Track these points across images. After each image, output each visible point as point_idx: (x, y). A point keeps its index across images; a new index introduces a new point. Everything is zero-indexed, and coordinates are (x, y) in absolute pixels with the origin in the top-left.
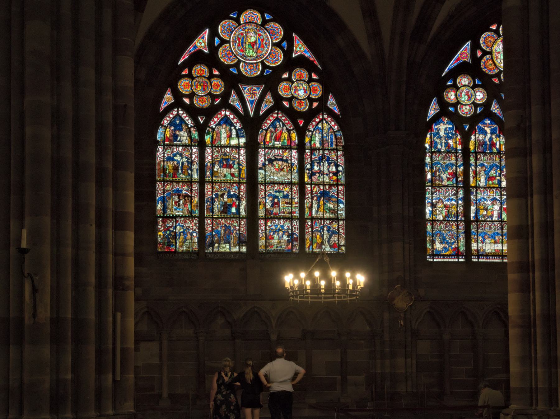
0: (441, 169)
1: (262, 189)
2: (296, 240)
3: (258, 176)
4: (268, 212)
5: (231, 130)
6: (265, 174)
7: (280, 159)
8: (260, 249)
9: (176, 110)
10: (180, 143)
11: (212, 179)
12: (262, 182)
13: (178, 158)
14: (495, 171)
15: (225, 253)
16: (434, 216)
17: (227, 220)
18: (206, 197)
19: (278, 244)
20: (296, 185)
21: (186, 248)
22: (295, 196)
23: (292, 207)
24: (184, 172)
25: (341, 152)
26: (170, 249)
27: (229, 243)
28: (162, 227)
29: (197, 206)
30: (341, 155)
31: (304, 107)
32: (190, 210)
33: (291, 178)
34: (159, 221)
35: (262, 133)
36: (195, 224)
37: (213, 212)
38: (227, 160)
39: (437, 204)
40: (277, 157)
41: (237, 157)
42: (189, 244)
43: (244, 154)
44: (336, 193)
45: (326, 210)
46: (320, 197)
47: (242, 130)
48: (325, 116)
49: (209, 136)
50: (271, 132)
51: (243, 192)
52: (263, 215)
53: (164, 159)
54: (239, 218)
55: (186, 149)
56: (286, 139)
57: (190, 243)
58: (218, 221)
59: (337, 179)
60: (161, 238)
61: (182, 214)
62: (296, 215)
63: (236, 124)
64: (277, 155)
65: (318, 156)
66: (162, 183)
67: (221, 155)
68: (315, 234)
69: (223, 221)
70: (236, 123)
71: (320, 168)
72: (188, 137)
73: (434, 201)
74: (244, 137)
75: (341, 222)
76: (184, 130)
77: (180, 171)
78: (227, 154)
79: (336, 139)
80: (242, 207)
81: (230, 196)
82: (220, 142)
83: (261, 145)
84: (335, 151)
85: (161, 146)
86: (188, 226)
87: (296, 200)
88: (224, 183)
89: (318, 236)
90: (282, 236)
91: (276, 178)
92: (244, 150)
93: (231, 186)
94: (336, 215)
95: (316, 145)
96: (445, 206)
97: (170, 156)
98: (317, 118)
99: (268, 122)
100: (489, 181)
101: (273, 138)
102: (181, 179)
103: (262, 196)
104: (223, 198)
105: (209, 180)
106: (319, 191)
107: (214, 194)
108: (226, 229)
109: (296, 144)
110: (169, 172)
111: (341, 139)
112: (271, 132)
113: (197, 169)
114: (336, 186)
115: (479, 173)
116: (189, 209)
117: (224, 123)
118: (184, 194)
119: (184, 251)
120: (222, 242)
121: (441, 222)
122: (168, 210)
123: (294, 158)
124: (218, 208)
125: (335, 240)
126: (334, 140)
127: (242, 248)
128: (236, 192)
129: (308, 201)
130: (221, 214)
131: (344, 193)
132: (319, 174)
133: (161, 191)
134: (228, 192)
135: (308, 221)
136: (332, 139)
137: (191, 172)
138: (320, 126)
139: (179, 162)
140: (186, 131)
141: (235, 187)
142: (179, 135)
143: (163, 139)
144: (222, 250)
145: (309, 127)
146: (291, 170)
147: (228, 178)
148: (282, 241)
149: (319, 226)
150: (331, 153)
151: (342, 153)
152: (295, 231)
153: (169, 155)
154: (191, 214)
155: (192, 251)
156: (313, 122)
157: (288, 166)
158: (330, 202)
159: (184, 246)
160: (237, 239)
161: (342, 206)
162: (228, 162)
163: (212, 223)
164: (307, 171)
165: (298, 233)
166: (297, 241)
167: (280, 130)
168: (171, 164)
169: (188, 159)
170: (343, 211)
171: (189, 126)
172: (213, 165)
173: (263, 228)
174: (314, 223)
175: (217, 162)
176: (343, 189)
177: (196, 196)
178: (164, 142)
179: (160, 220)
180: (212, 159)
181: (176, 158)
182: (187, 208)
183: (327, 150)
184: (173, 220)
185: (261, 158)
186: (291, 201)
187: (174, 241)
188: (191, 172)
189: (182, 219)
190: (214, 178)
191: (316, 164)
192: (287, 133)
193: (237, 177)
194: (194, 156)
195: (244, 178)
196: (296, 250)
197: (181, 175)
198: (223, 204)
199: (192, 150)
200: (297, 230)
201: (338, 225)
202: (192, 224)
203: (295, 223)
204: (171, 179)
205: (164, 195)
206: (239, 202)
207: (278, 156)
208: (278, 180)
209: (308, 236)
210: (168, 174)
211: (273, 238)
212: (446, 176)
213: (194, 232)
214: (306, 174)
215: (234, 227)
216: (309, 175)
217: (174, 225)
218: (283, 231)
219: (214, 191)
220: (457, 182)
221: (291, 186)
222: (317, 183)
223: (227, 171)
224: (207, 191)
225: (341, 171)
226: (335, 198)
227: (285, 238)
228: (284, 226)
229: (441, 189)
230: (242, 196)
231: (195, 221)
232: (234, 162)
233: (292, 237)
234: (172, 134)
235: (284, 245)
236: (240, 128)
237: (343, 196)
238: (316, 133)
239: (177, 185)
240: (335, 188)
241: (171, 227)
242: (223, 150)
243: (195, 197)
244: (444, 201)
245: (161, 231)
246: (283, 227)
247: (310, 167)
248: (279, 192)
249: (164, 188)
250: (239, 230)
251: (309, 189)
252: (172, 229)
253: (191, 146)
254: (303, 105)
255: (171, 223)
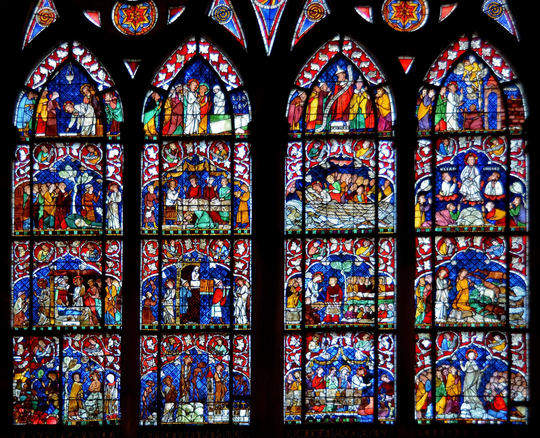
1: (294, 252)
2: (388, 389)
3: (283, 219)
4: (311, 315)
5: (211, 95)
6: (304, 211)
7: (345, 166)
8: (287, 415)
9: (65, 46)
10: (75, 134)
11: (160, 230)
12: (294, 232)
13: (68, 174)
15: (192, 427)
17: (197, 337)
18: (144, 277)
19: (338, 401)
20: (390, 239)
21: (89, 415)
22: (385, 270)
23: (376, 299)
24: (86, 213)
25: (520, 142)
26: (45, 420)
27: (204, 400)
28: (23, 359)
29: (118, 303)
30: (519, 150)
31: (415, 18)
32: (100, 312)
33: (377, 220)
34: (17, 344)
35: (297, 100)
36: (113, 349)
37: (160, 318)
38: (199, 175)
40: (336, 163)
41: (228, 167)
42: (97, 404)
43: (247, 159)
44: (503, 258)
45: (475, 305)
46: (458, 270)
47: (243, 94)
48: (476, 44)
49: (151, 113)
50: (322, 95)
51: (242, 262)
52: (297, 323)
53: (31, 178)
54: (231, 332)
55: (91, 150)
56: (364, 111)
57: (100, 402)
58: (173, 341)
59: (508, 214)
60: (21, 389)
61: (78, 323)
62: (390, 320)
63: (227, 78)
64: (337, 156)
65: (453, 152)
66: (27, 243)
67: (183, 164)
68: (442, 371)
69: (188, 339)
70: (226, 75)
71: (458, 188)
72: (97, 118)
74: (247, 112)
75: (517, 339)
76: (86, 100)
77: (74, 211)
78: (201, 158)
79: (506, 104)
80: (239, 304)
81: (205, 274)
82: (183, 126)
83: (292, 131)
84: (503, 138)
85: (26, 143)
86: (93, 357)
87: (390, 280)
88: (192, 238)
89: (451, 378)
90: (350, 380)
91: (334, 221)
92: (245, 148)
93: (211, 247)
94: (503, 317)
95: (448, 126)
97: (48, 170)
98: (452, 49)
99: (315, 67)
101: (327, 111)
102: (76, 233)
103: (295, 270)
104: (189, 279)
105: (150, 232)
106: (453, 252)
107: (165, 271)
108: (194, 362)
109: (391, 126)
110: (46, 214)
111: (520, 105)
112: (322, 95)
113: (118, 204)
114: (502, 238)
116: (96, 312)
117: (196, 77)
118: (85, 272)
119: (82, 424)
120: (184, 398)
122: (43, 316)
123: (386, 164)
124: (174, 306)
125: (500, 387)
126: (499, 109)
127: (239, 414)
128: (222, 262)
129: (422, 282)
130: (182, 322)
131: (525, 258)
132: (456, 206)
133: (22, 265)
134: (201, 263)
135: (422, 336)
136: (493, 106)
137: (105, 213)
138: (458, 72)
139: (73, 186)
140: (91, 103)
141: (222, 248)
142: (72, 113)
143: (31, 127)
144: (184, 420)
145: (429, 75)
146: (375, 196)
147: (203, 225)
148: (349, 393)
149: (454, 349)
150: (492, 144)
151: (523, 143)
152: (384, 365)
153: (45, 166)
154: (102, 324)
155: (104, 422)
156: (440, 63)
157: (369, 184)
158: (487, 284)
159: (83, 411)
160: (226, 389)
161: (519, 292)
162: (202, 182)
163: (158, 347)
164: (422, 200)
165: (393, 371)
166: (390, 393)
167: (346, 88)
168: (51, 191)
169: (96, 177)
170: (522, 305)
171: (100, 88)
172: (162, 190)
173: (297, 358)
174: (441, 342)
175: (173, 183)
176: (525, 244)
177: (117, 275)
178: (32, 133)
179: (19, 341)
180: (159, 176)
181: (63, 175)
182: (93, 309)
183: (480, 137)
184: (54, 341)
185: (293, 167)
186: (373, 281)
187: (55, 397)
188: (105, 213)
189: (78, 337)
190: (165, 227)
191: (447, 177)
192: (365, 95)
193: (227, 222)
194: (111, 170)
195: (247, 224)
196: (388, 416)
197: (76, 222)
198: (189, 295)
199: (106, 152)
200: (392, 362)
201: (509, 344)
202: (104, 352)
203: (387, 344)
204: (50, 233)
205: (31, 274)
206: (231, 291)
207: (341, 158)
208: (339, 227)
209: (422, 377)
210: (43, 217)
211: (323, 385)
213: (110, 373)
214: (417, 207)
215: (215, 356)
216: (427, 209)
217: (56, 352)
218: (351, 366)
219: (165, 261)
221: (376, 242)
222: (448, 230)
223: (199, 206)
224: (145, 260)
225: (519, 195)
226: (499, 271)
227: (358, 383)
228: (354, 351)
230: (240, 273)
231: (111, 343)
232: (218, 181)
233: (376, 382)
234: (54, 112)
235: (355, 403)
236: (236, 87)
237: (524, 263)
238: (448, 91)
239: (65, 250)
240: (500, 242)
241: (47, 359)
242: (190, 149)
243: (113, 279)
245: (21, 371)
246: (351, 353)
247: (430, 188)
248: (342, 258)
249: (31, 257)
250: (231, 364)
251: (426, 248)
252: (50, 365)
253: (104, 141)
254: (411, 16)
255: (48, 349)
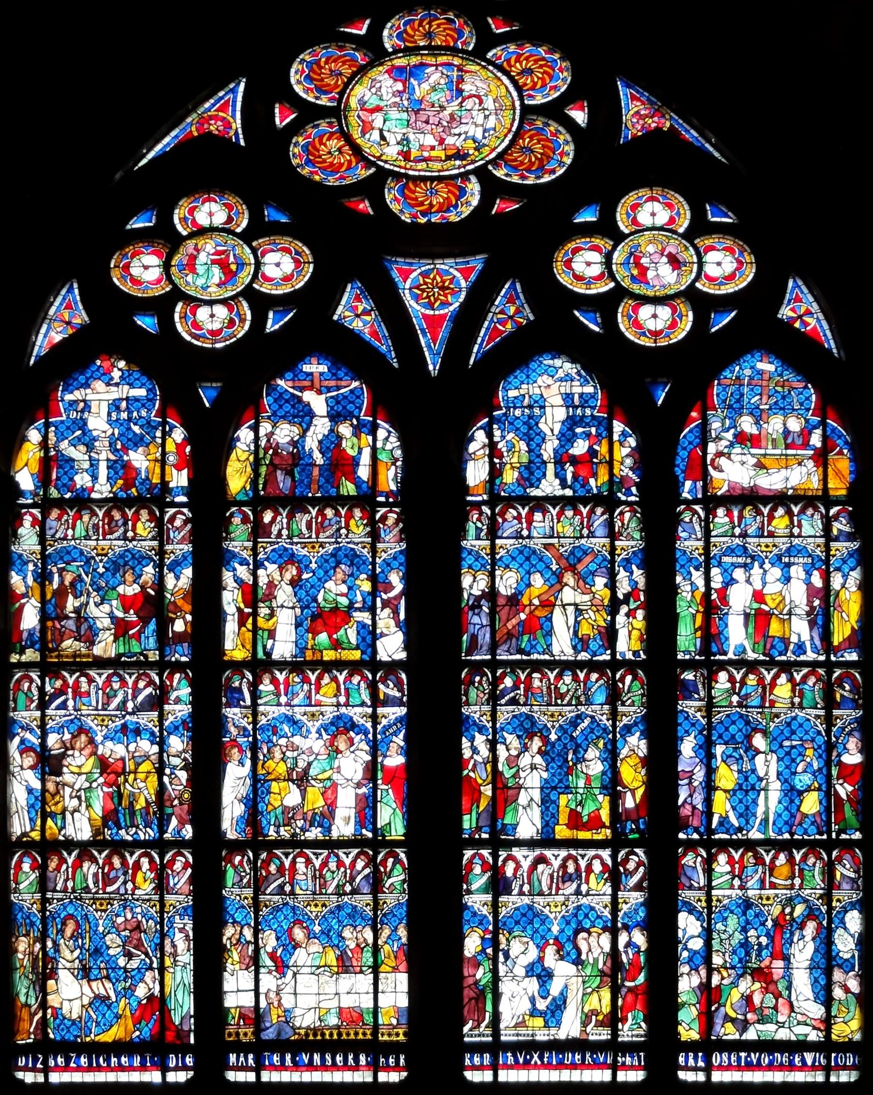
0: (87, 580)
14: (344, 582)
16: (50, 822)
39: (63, 756)
73: (52, 740)
96: (104, 764)
100: (315, 633)
115: (270, 596)
121: (84, 850)
212: (111, 616)
220: (163, 639)
229: (87, 676)
244: (99, 738)
